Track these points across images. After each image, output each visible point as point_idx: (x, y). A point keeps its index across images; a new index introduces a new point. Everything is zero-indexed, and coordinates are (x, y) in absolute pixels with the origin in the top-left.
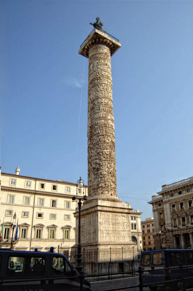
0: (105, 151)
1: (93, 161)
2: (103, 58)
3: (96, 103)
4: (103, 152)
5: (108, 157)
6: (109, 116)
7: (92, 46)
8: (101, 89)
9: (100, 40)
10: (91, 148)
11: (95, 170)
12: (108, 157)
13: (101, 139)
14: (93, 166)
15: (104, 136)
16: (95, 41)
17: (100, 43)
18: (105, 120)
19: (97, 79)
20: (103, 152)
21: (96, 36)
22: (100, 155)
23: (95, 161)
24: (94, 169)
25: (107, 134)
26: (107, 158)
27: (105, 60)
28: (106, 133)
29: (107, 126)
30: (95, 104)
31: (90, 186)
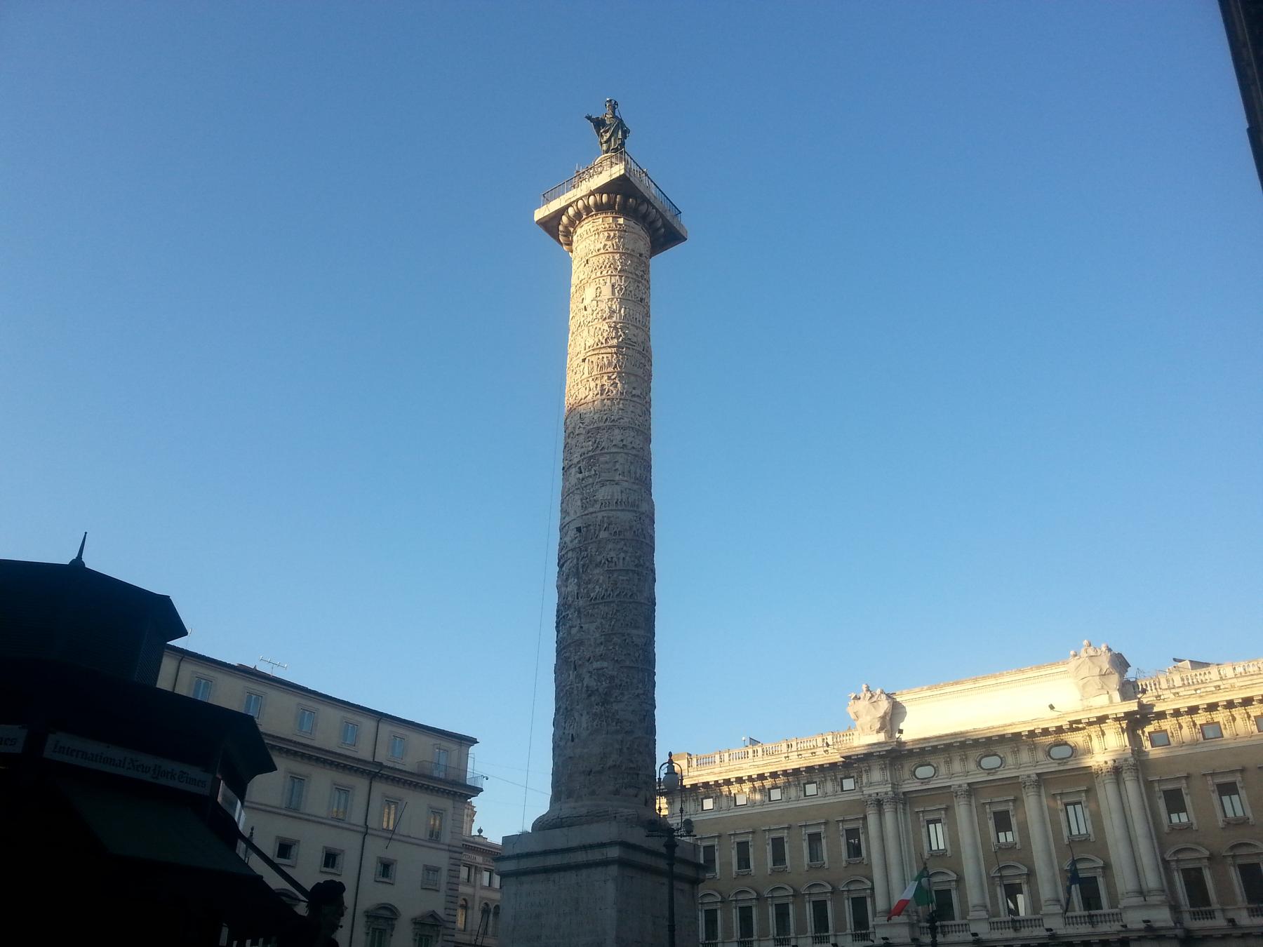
0: (634, 632)
1: (587, 664)
10: (579, 612)
11: (593, 699)
15: (631, 574)
23: (596, 665)
24: (590, 696)
27: (639, 282)
28: (636, 566)
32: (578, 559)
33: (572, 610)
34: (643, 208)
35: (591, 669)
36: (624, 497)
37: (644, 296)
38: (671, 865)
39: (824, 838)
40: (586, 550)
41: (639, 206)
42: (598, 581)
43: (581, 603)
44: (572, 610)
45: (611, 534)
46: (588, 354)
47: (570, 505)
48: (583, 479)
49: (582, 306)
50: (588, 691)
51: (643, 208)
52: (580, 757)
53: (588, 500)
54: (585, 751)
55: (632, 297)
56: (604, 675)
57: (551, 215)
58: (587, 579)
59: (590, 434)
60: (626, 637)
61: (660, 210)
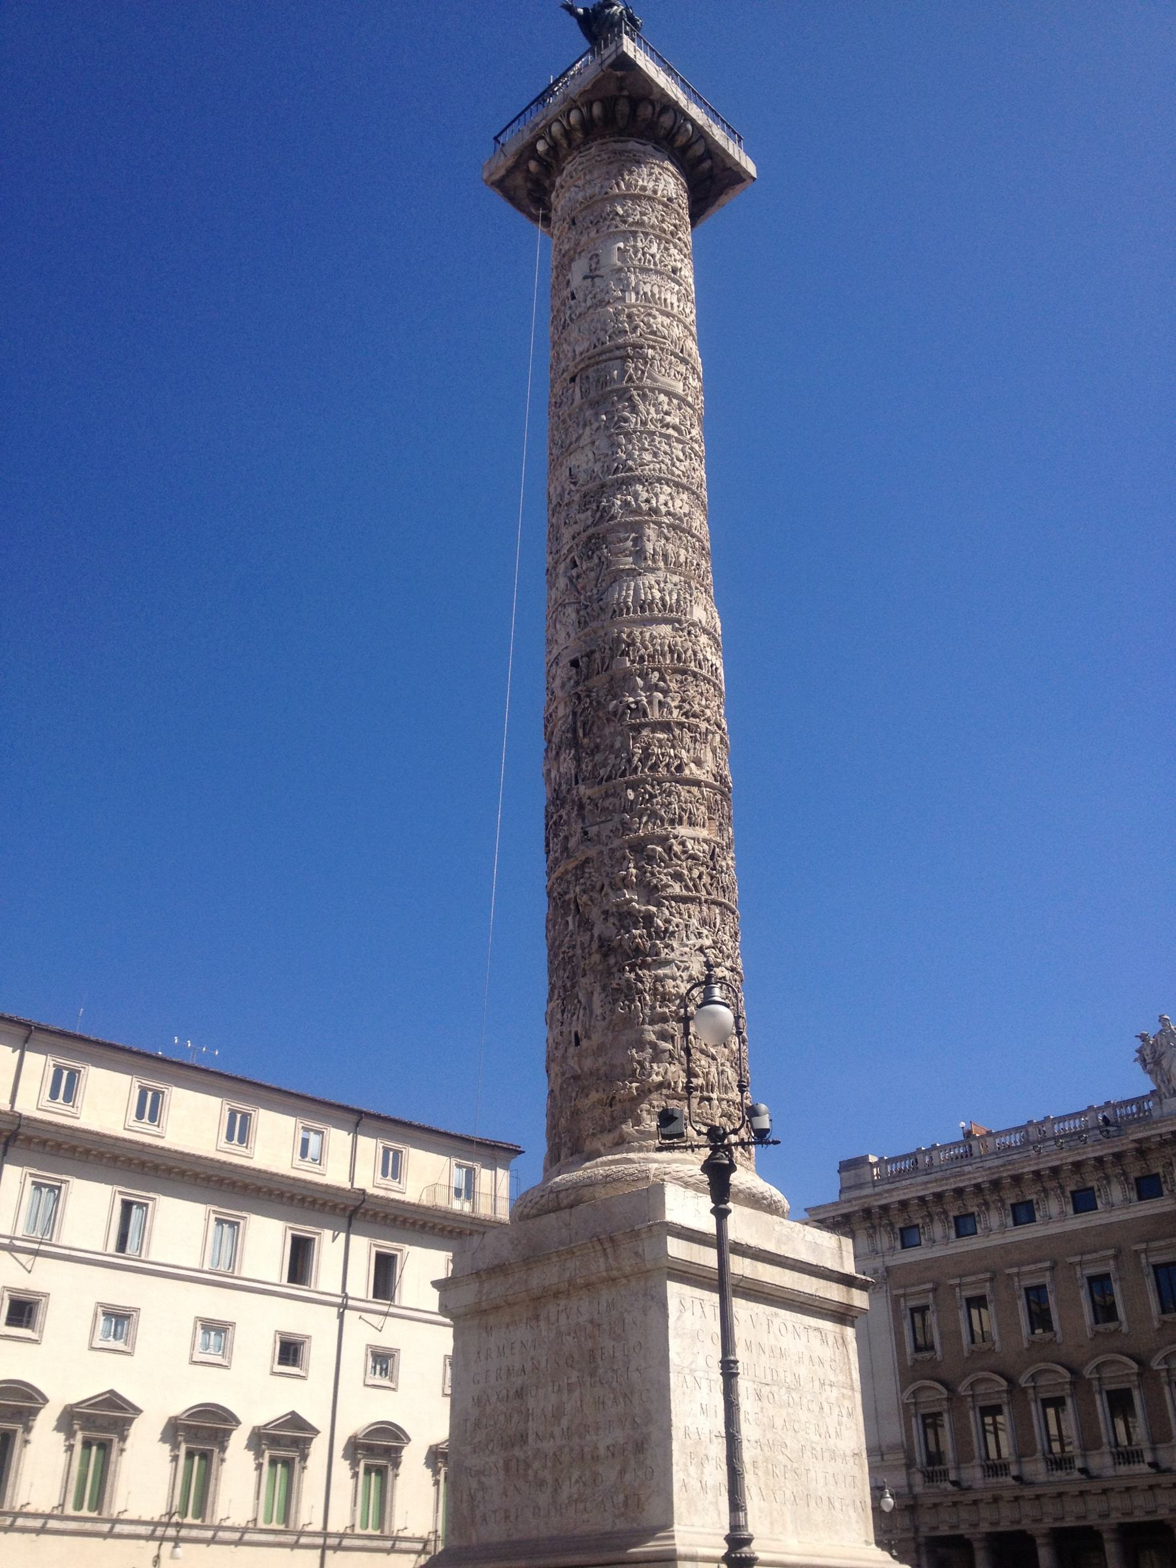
0: (683, 831)
2: (653, 227)
4: (667, 838)
5: (700, 877)
6: (701, 608)
8: (651, 427)
11: (612, 961)
12: (700, 877)
13: (657, 750)
15: (677, 732)
16: (605, 109)
18: (675, 629)
19: (618, 353)
20: (667, 838)
21: (622, 79)
22: (651, 859)
24: (605, 956)
26: (695, 886)
28: (686, 714)
29: (692, 666)
31: (576, 1078)
32: (574, 714)
34: (667, 120)
37: (679, 265)
38: (721, 1214)
39: (1115, 1280)
40: (588, 696)
41: (658, 117)
42: (612, 746)
44: (568, 807)
47: (558, 626)
48: (578, 577)
49: (566, 293)
50: (601, 946)
51: (667, 120)
52: (591, 1073)
53: (589, 610)
54: (601, 1060)
55: (655, 264)
57: (510, 162)
59: (587, 499)
60: (672, 840)
61: (700, 123)
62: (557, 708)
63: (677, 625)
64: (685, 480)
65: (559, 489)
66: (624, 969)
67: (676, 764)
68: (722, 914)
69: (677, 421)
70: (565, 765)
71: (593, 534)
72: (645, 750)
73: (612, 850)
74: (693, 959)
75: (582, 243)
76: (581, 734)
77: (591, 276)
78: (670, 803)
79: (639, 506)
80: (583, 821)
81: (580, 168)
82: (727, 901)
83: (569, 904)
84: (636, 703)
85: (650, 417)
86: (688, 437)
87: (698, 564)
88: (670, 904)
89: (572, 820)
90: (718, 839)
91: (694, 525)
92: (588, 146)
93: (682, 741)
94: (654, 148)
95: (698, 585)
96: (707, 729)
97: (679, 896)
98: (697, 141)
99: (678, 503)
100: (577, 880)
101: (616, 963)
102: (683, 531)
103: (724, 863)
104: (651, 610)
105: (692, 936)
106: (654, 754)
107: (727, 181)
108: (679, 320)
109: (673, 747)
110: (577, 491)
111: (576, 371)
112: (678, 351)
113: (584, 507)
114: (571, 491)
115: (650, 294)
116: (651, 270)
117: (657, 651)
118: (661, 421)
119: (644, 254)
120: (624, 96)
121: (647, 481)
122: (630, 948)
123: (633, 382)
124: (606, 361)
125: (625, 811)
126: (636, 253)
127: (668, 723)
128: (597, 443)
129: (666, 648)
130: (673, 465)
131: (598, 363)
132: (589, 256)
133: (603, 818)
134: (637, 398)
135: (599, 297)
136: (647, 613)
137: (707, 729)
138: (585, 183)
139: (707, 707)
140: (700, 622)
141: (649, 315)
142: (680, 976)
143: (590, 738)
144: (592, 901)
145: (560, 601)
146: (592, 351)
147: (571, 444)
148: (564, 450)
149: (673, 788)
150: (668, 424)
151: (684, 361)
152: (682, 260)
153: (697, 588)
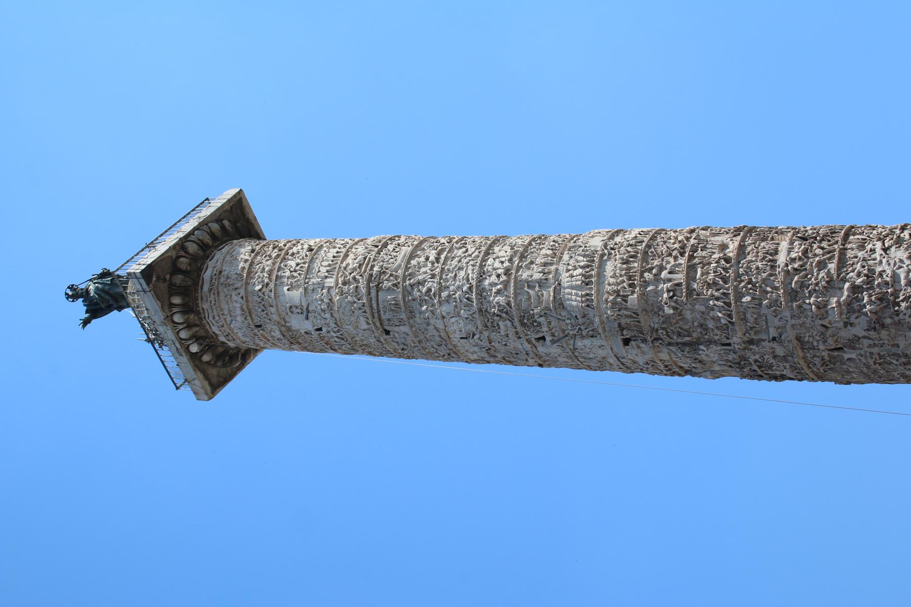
0: (782, 259)
2: (274, 264)
3: (500, 299)
5: (823, 248)
6: (591, 240)
7: (198, 313)
9: (183, 267)
10: (751, 342)
11: (888, 321)
12: (823, 248)
13: (711, 276)
14: (865, 334)
15: (696, 261)
17: (199, 270)
19: (373, 294)
21: (158, 278)
22: (802, 285)
24: (883, 326)
25: (688, 250)
26: (829, 252)
28: (682, 254)
29: (641, 247)
30: (509, 304)
32: (670, 344)
33: (748, 354)
34: (192, 248)
35: (841, 324)
36: (579, 271)
37: (306, 247)
42: (703, 313)
43: (736, 339)
44: (748, 354)
45: (633, 292)
46: (378, 324)
47: (591, 356)
48: (553, 335)
49: (315, 334)
50: (875, 329)
53: (582, 328)
55: (304, 263)
56: (849, 305)
57: (201, 376)
58: (699, 330)
59: (489, 324)
61: (196, 224)
62: (661, 360)
63: (605, 258)
64: (483, 249)
65: (476, 349)
66: (896, 311)
67: (723, 263)
68: (854, 234)
69: (434, 252)
70: (712, 355)
71: (520, 321)
72: (709, 286)
73: (792, 317)
74: (892, 256)
75: (278, 319)
76: (688, 339)
77: (306, 312)
78: (757, 268)
79: (502, 282)
80: (763, 340)
81: (217, 318)
82: (843, 232)
83: (834, 357)
84: (668, 291)
85: (428, 271)
86: (447, 244)
87: (554, 241)
88: (845, 272)
89: (761, 350)
90: (790, 235)
91: (520, 243)
92: (201, 311)
93: (705, 257)
94: (210, 260)
95: (572, 242)
96: (695, 239)
97: (838, 264)
98: (209, 228)
99: (502, 253)
100: (814, 348)
101: (891, 318)
102: (526, 250)
103: (810, 232)
104: (591, 276)
105: (873, 256)
106: (714, 279)
107: (239, 212)
108: (351, 247)
109: (709, 264)
110: (481, 333)
111: (381, 330)
112: (376, 249)
113: (496, 328)
114: (479, 339)
115: (328, 268)
116: (309, 266)
117: (626, 273)
118: (433, 263)
119: (295, 271)
120: (170, 277)
121: (481, 276)
122: (879, 305)
123: (399, 283)
124: (378, 304)
125: (760, 304)
126: (293, 277)
127: (688, 267)
128: (444, 314)
129: (625, 266)
130: (470, 255)
131: (379, 311)
132: (289, 313)
133: (764, 323)
134: (412, 281)
135: (324, 306)
136: (593, 280)
137: (695, 239)
138: (231, 316)
139: (676, 238)
140: (603, 241)
141: (345, 268)
142: (907, 266)
143: (693, 331)
144: (834, 336)
145: (571, 353)
146: (368, 315)
147: (440, 336)
148: (444, 343)
149: (745, 265)
150: (436, 258)
151: (385, 245)
152: (302, 244)
153: (575, 242)
